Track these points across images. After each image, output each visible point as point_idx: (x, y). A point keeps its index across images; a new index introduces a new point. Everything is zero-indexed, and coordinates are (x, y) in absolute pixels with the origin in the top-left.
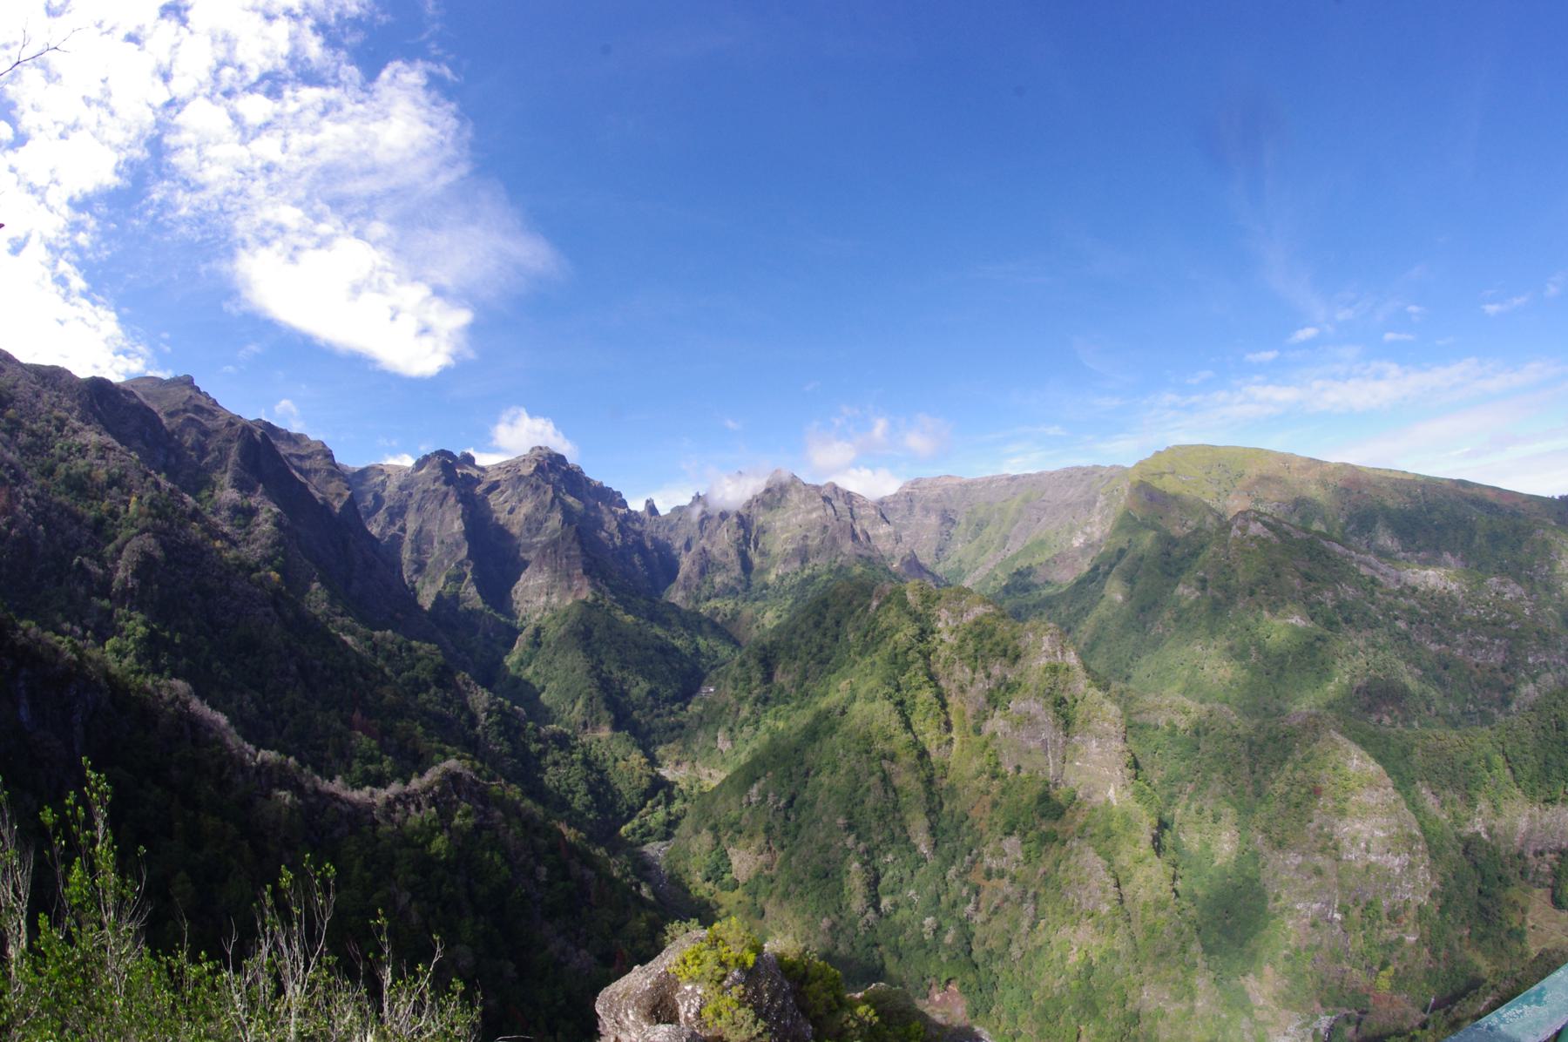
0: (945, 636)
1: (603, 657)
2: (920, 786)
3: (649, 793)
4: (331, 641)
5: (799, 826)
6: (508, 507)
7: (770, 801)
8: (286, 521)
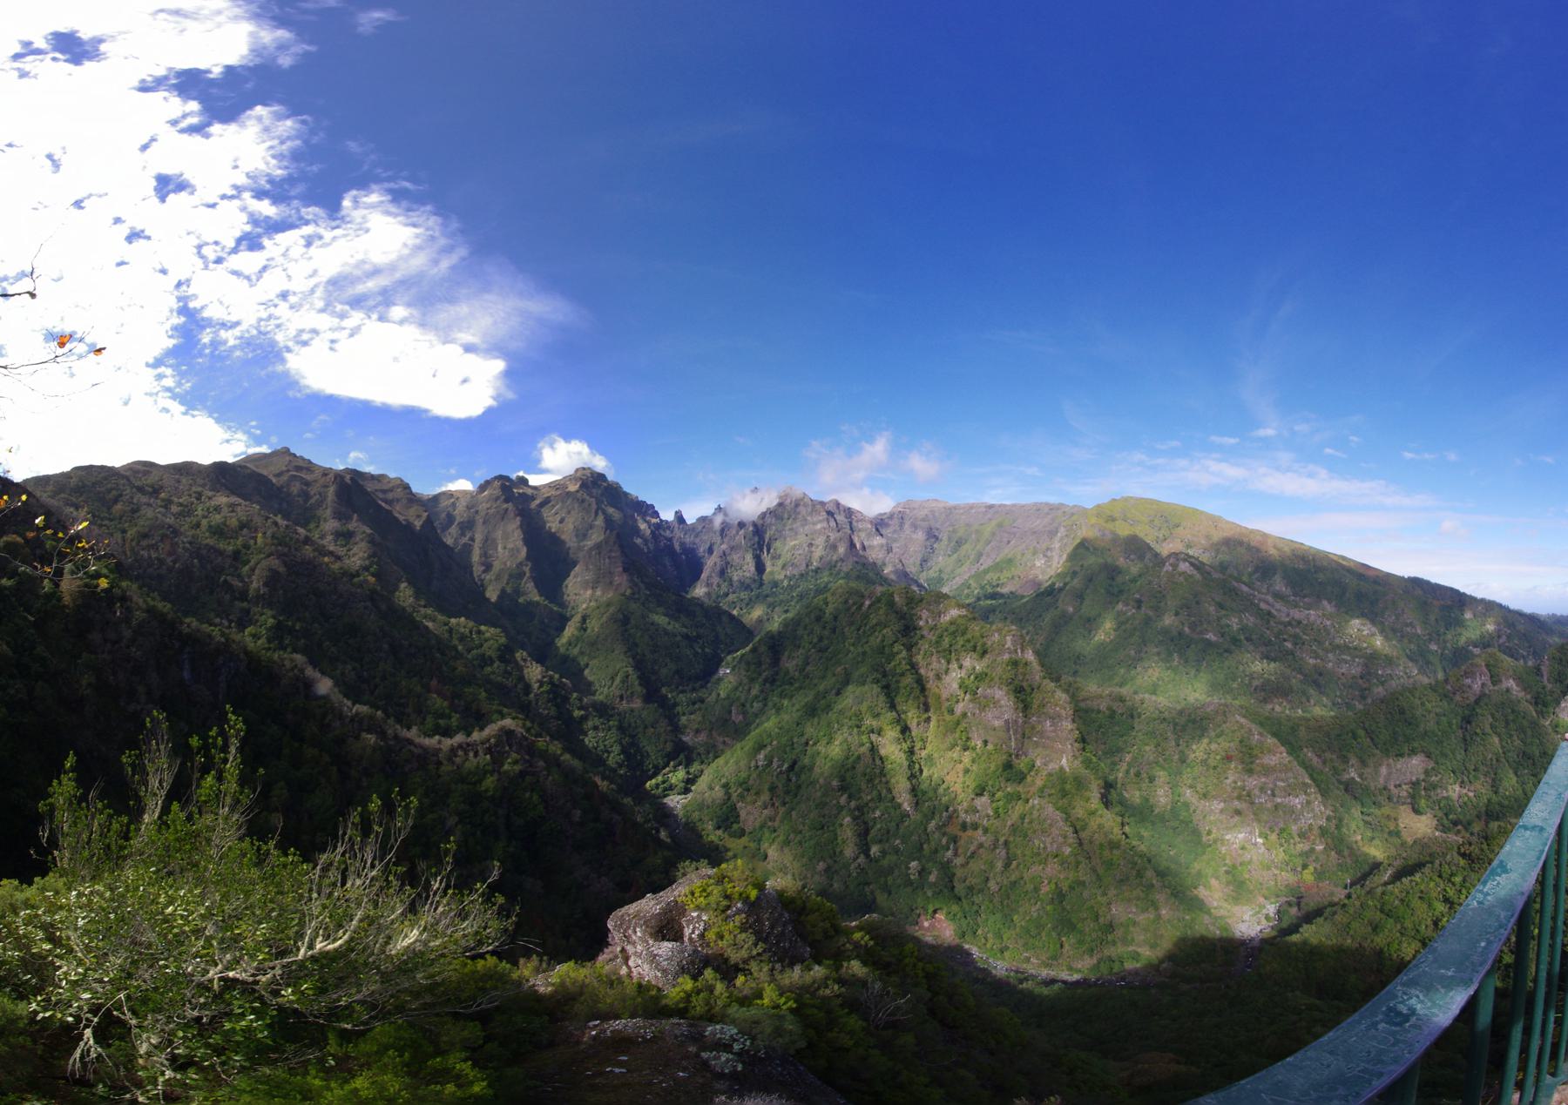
0: (925, 633)
4: (416, 626)
5: (799, 787)
6: (558, 518)
7: (775, 765)
8: (378, 538)
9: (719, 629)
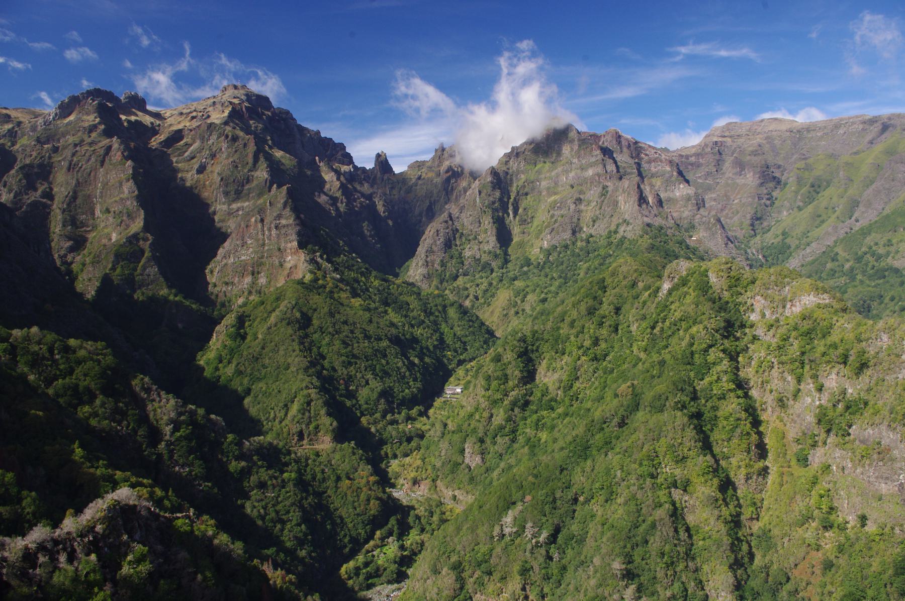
0: (760, 332)
1: (324, 350)
2: (724, 529)
3: (377, 522)
5: (564, 568)
7: (528, 533)
9: (444, 327)
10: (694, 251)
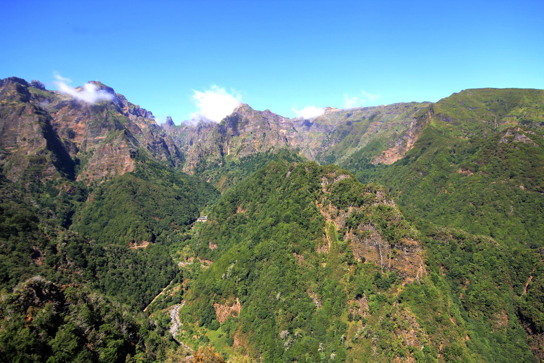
0: (324, 190)
10: (300, 159)
